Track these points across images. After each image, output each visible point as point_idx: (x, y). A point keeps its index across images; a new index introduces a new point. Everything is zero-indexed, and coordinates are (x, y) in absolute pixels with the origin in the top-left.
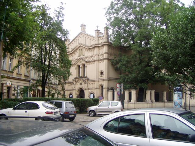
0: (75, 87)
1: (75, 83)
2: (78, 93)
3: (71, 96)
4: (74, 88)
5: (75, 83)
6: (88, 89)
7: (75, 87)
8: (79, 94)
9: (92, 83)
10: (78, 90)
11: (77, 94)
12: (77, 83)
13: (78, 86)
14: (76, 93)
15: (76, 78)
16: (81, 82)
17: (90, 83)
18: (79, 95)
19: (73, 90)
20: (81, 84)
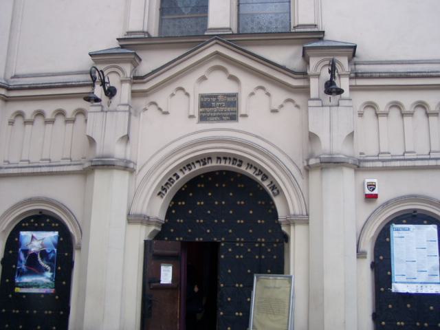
0: (126, 138)
1: (124, 92)
2: (158, 209)
3: (50, 237)
4: (119, 152)
5: (124, 92)
6: (358, 166)
7: (126, 138)
8: (162, 218)
9: (408, 100)
10: (188, 165)
11: (144, 220)
12: (162, 98)
13: (164, 134)
14: (140, 208)
15: (132, 46)
16: (218, 84)
17: (382, 100)
18: (158, 236)
19: (106, 164)
20: (218, 108)
